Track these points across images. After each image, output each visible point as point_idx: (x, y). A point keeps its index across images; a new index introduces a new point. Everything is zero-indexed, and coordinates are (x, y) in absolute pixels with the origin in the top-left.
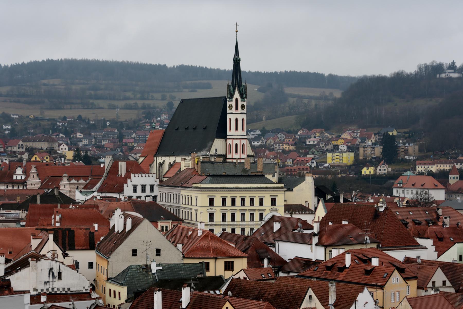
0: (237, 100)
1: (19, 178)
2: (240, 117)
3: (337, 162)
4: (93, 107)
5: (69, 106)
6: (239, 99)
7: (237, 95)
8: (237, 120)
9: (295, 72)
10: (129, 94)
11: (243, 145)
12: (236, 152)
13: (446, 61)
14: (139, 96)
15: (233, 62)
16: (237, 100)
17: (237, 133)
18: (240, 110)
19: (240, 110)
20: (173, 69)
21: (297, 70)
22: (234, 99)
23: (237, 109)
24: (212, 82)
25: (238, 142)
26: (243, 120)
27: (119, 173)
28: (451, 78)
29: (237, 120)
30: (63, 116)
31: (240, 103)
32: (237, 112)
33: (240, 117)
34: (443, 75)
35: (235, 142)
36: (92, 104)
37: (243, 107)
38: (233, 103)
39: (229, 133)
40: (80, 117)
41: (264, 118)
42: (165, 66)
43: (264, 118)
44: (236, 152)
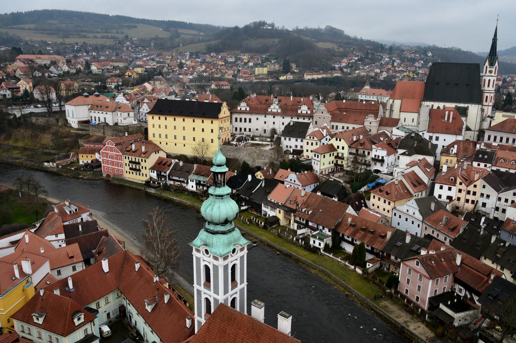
1: (304, 112)
2: (492, 79)
3: (260, 72)
4: (85, 37)
5: (72, 36)
6: (488, 67)
8: (489, 80)
9: (173, 21)
10: (99, 30)
13: (269, 22)
14: (104, 31)
15: (242, 21)
20: (113, 17)
21: (170, 20)
22: (494, 67)
24: (137, 25)
27: (446, 119)
28: (268, 29)
29: (489, 80)
30: (76, 42)
34: (265, 27)
36: (85, 35)
38: (493, 70)
39: (486, 88)
40: (84, 43)
41: (181, 45)
42: (108, 15)
43: (181, 45)
44: (486, 101)
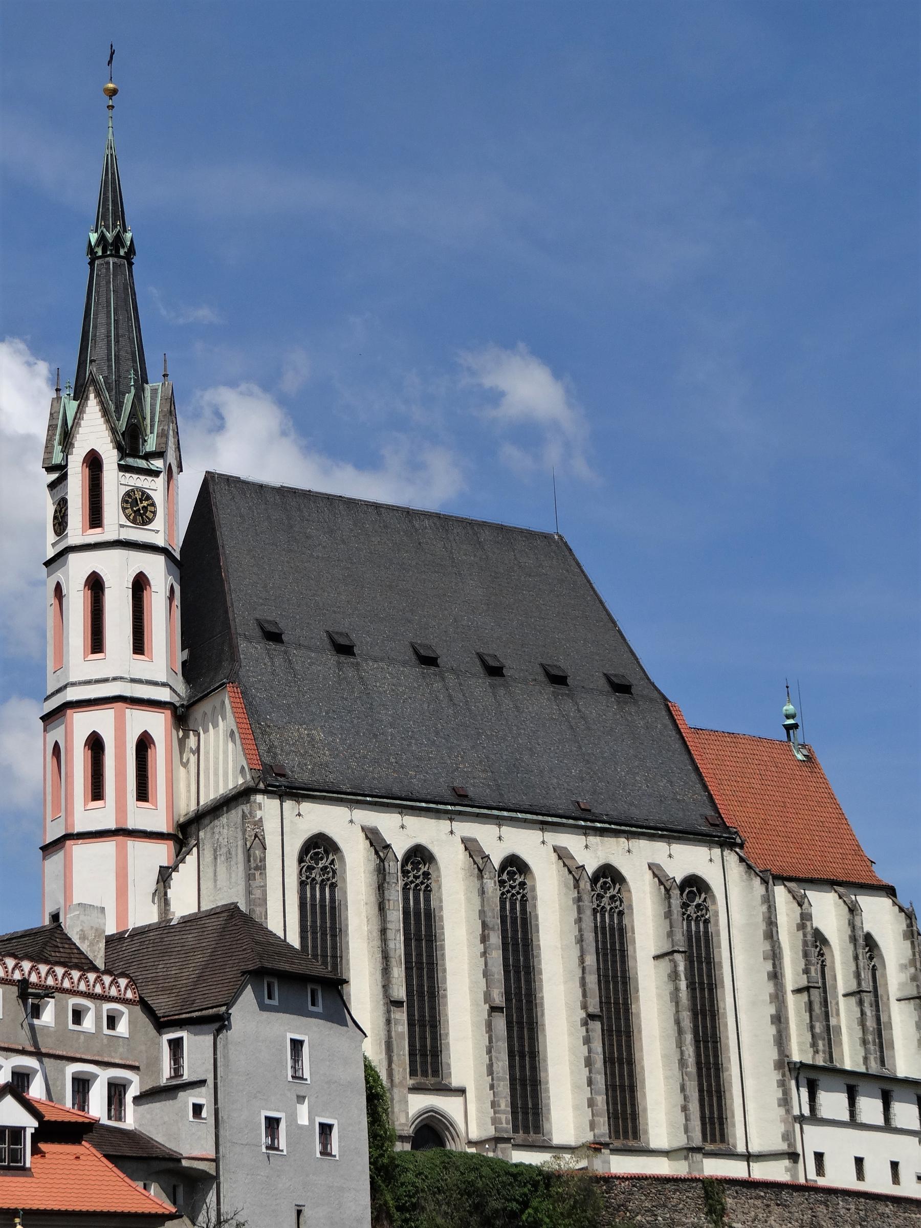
0: (94, 462)
7: (94, 433)
11: (144, 744)
12: (97, 792)
16: (94, 462)
17: (97, 667)
18: (115, 522)
19: (115, 522)
23: (95, 518)
25: (101, 721)
26: (140, 584)
31: (115, 484)
32: (95, 536)
33: (117, 570)
35: (83, 724)
37: (138, 508)
